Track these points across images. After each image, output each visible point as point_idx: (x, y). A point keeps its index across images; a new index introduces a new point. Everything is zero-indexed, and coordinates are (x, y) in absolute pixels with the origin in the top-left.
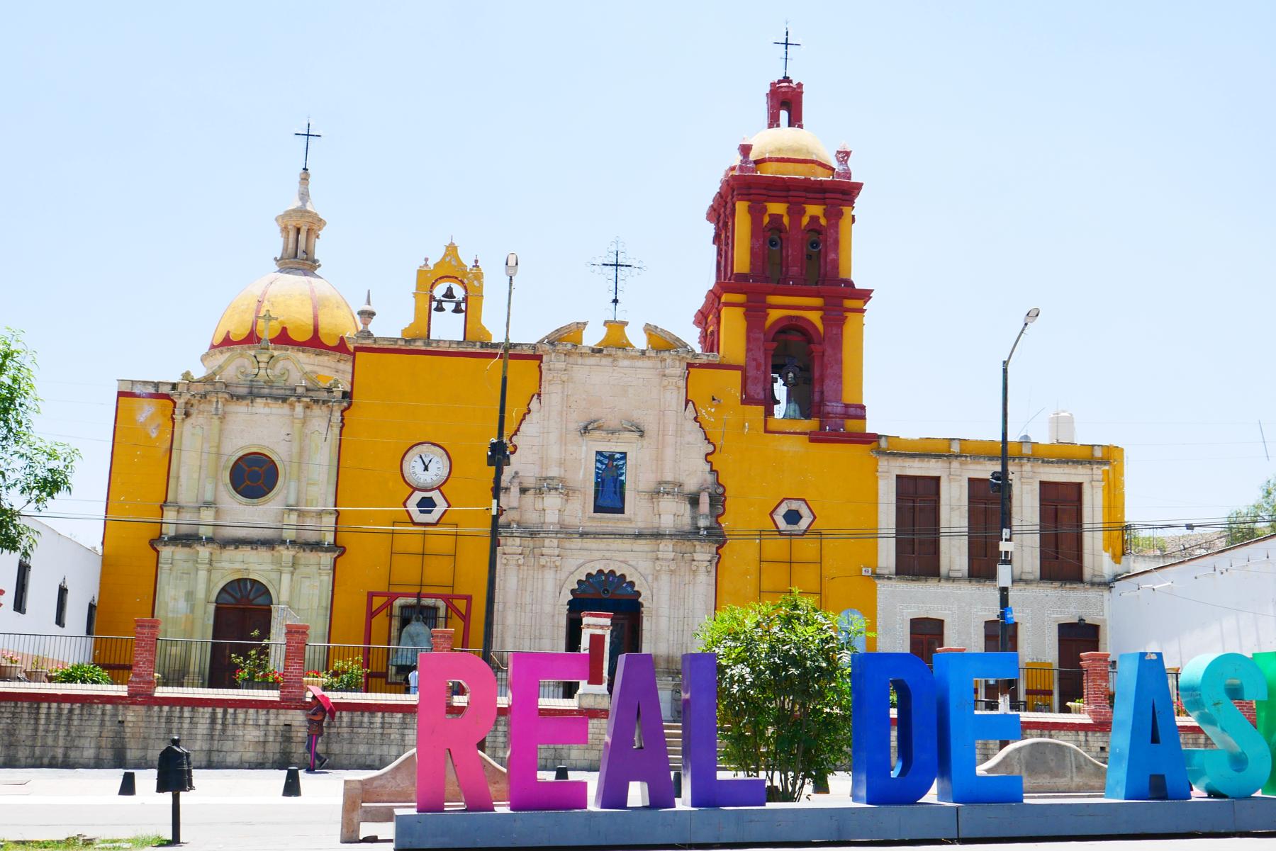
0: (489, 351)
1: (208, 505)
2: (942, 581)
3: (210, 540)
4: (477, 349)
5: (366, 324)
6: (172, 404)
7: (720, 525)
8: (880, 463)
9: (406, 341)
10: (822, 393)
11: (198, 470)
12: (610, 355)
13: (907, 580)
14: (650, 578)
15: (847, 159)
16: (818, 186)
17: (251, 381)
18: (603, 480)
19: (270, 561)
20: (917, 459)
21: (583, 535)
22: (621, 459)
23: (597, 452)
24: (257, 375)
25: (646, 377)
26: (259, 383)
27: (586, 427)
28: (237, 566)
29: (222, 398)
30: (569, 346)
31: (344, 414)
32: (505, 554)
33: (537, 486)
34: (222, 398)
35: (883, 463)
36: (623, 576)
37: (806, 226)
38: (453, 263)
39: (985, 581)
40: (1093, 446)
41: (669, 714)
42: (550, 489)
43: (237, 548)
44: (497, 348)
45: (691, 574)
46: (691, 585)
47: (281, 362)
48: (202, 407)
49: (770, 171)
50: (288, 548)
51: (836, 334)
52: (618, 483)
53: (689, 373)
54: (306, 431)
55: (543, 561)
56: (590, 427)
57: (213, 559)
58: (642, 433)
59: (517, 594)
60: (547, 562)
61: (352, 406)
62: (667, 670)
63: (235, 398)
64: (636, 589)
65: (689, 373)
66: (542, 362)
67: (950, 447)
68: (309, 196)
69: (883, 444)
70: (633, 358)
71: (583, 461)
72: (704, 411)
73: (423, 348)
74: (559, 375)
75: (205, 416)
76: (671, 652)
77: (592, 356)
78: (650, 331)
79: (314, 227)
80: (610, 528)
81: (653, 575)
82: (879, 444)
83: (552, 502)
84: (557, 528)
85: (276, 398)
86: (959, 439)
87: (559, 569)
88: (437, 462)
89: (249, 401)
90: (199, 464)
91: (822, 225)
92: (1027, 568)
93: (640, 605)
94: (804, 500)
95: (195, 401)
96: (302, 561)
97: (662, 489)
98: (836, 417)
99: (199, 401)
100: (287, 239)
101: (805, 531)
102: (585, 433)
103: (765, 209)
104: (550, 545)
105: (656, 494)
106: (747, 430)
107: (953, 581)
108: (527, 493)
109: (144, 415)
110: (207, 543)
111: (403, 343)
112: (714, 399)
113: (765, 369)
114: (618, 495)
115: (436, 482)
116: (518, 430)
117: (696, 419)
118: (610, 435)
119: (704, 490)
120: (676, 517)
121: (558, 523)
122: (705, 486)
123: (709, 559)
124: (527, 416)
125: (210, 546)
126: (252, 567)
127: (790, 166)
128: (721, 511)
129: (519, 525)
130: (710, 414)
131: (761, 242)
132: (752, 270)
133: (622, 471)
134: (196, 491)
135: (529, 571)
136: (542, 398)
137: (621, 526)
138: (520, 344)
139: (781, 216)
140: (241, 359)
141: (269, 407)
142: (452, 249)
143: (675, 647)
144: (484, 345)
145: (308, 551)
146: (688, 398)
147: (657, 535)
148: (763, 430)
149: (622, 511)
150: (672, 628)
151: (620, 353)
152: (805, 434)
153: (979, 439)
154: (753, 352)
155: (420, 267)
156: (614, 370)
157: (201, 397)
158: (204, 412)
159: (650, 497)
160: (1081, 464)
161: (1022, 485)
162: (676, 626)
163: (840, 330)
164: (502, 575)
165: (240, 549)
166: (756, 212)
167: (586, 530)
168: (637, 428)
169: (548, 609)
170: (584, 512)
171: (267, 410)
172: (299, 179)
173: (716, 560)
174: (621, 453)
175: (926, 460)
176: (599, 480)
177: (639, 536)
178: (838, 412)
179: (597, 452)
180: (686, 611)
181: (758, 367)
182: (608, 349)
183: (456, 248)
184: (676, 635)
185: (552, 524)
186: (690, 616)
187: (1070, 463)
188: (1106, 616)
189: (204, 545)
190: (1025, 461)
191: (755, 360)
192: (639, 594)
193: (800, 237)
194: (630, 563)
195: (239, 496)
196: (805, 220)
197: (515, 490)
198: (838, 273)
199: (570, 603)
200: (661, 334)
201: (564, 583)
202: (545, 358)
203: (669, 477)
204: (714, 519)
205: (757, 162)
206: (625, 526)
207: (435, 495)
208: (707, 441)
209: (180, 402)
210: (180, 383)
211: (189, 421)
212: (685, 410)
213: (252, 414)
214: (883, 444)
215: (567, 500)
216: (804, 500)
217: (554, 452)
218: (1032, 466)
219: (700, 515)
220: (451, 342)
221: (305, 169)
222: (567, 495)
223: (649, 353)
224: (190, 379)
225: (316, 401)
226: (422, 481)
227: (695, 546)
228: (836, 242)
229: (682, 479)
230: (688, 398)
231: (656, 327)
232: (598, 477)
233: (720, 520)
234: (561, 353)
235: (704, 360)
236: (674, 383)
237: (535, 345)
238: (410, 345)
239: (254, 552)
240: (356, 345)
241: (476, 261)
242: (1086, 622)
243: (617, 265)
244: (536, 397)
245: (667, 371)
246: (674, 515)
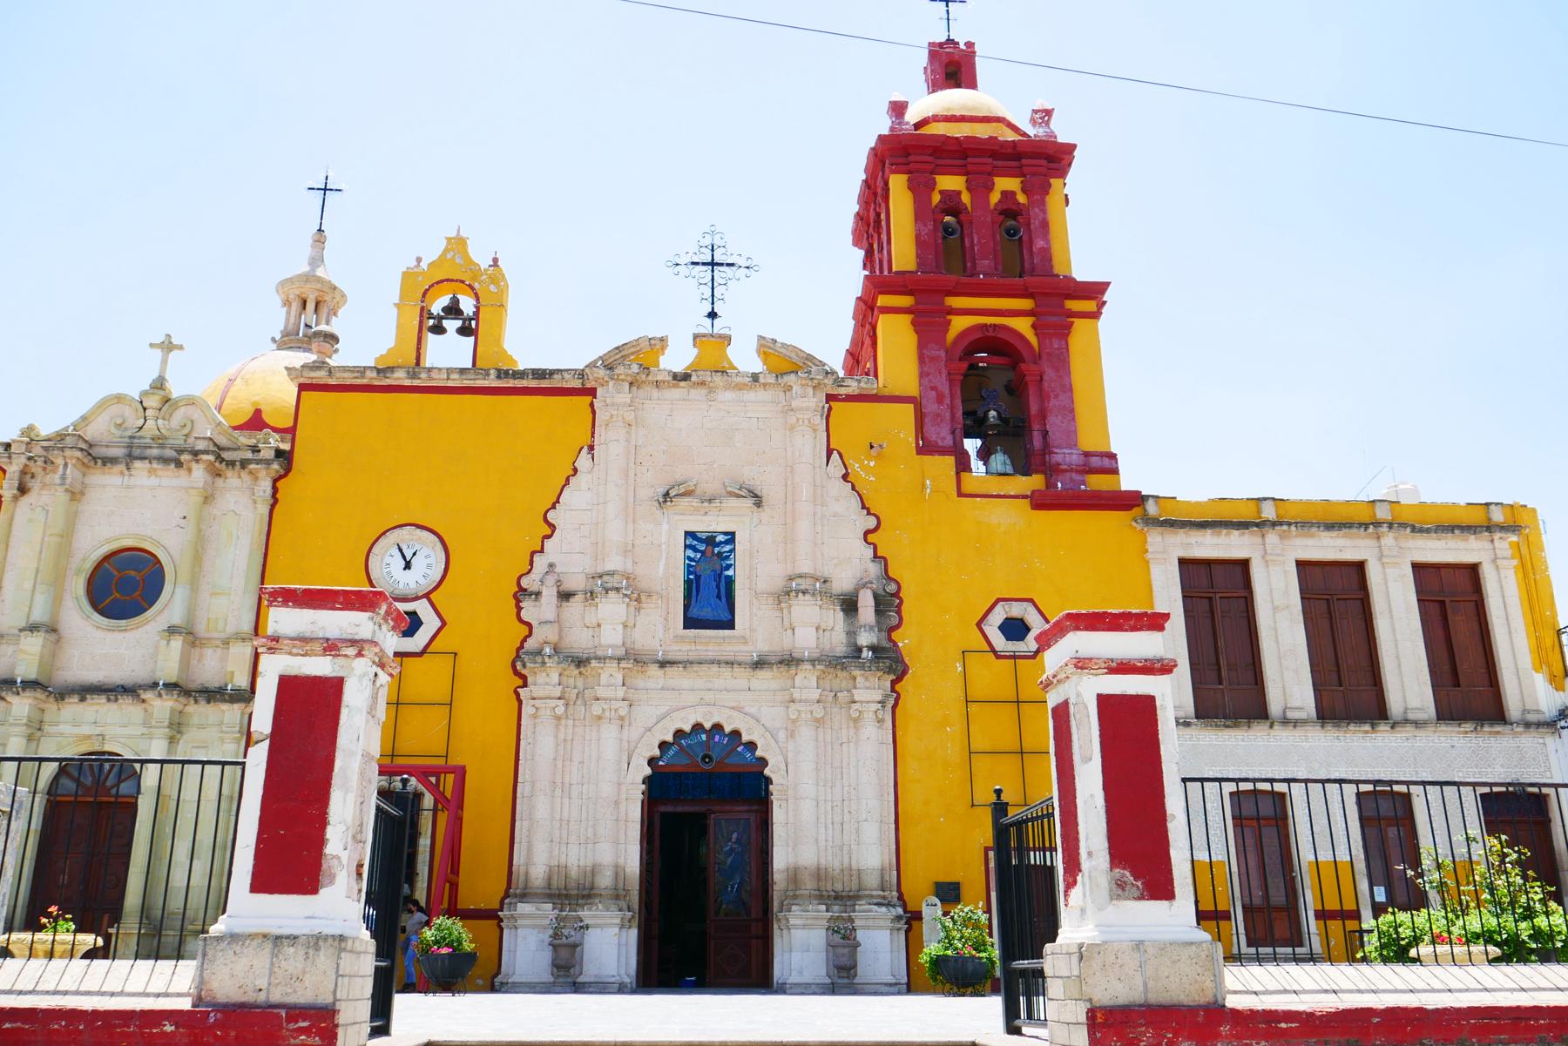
0: (511, 383)
1: (33, 628)
2: (1275, 727)
3: (31, 685)
4: (492, 382)
7: (895, 644)
8: (1149, 539)
9: (379, 371)
10: (1045, 434)
11: (33, 576)
12: (703, 383)
13: (1216, 726)
14: (782, 735)
16: (1009, 150)
17: (131, 437)
18: (698, 578)
19: (141, 722)
20: (1209, 531)
21: (663, 664)
22: (726, 542)
23: (687, 534)
24: (141, 428)
25: (763, 415)
27: (667, 494)
28: (86, 730)
29: (72, 458)
30: (635, 368)
31: (279, 484)
32: (534, 699)
33: (589, 588)
34: (72, 458)
36: (736, 734)
37: (996, 204)
38: (458, 261)
39: (1348, 724)
40: (1487, 504)
41: (824, 972)
42: (607, 590)
43: (83, 699)
44: (523, 378)
45: (851, 724)
46: (851, 744)
47: (183, 409)
48: (48, 479)
50: (160, 695)
51: (1057, 349)
52: (723, 580)
53: (830, 409)
54: (215, 511)
55: (596, 709)
56: (672, 493)
57: (45, 719)
58: (758, 500)
59: (555, 765)
60: (603, 709)
61: (290, 474)
62: (817, 893)
63: (99, 462)
64: (759, 753)
65: (830, 409)
67: (1259, 511)
68: (323, 261)
69: (1151, 508)
70: (740, 387)
71: (663, 546)
72: (857, 465)
73: (407, 382)
74: (621, 412)
76: (823, 862)
77: (675, 386)
78: (767, 348)
79: (326, 298)
80: (711, 654)
81: (786, 729)
82: (1145, 511)
83: (611, 610)
84: (621, 652)
85: (165, 460)
86: (1273, 499)
87: (627, 723)
88: (427, 557)
89: (122, 467)
90: (36, 566)
91: (1019, 203)
93: (768, 781)
94: (1031, 601)
95: (36, 468)
96: (195, 720)
97: (794, 585)
98: (1071, 470)
99: (44, 469)
102: (665, 501)
103: (935, 183)
104: (609, 677)
105: (786, 594)
106: (928, 491)
107: (1295, 727)
108: (571, 600)
110: (24, 690)
111: (374, 374)
112: (872, 447)
113: (951, 401)
114: (724, 599)
115: (424, 587)
116: (558, 501)
117: (845, 477)
118: (706, 504)
119: (864, 586)
120: (821, 631)
121: (623, 644)
122: (867, 580)
123: (880, 698)
125: (28, 693)
126: (110, 731)
128: (895, 621)
129: (556, 650)
130: (866, 469)
131: (931, 227)
132: (919, 265)
133: (728, 562)
134: (27, 609)
135: (577, 729)
136: (596, 452)
137: (728, 648)
139: (959, 193)
140: (120, 405)
141: (156, 476)
142: (457, 244)
143: (830, 852)
144: (502, 374)
145: (203, 703)
146: (832, 447)
147: (790, 661)
149: (730, 625)
150: (822, 820)
151: (718, 378)
152: (1024, 497)
153: (1304, 498)
154: (931, 377)
155: (408, 268)
156: (710, 406)
159: (776, 602)
160: (1475, 533)
161: (1384, 567)
162: (830, 816)
163: (1063, 343)
164: (529, 734)
165: (89, 701)
166: (920, 189)
167: (670, 657)
168: (749, 491)
169: (607, 790)
170: (666, 629)
171: (153, 481)
172: (311, 241)
173: (892, 701)
174: (726, 534)
175: (1225, 531)
176: (691, 577)
177: (759, 664)
178: (1073, 462)
179: (687, 534)
180: (846, 788)
181: (940, 400)
182: (699, 373)
184: (830, 831)
185: (613, 647)
186: (853, 797)
187: (1456, 531)
189: (18, 694)
190: (1384, 529)
191: (933, 388)
192: (763, 762)
193: (989, 220)
194: (747, 709)
195: (97, 616)
196: (995, 198)
197: (549, 594)
198: (1052, 267)
199: (648, 781)
200: (783, 351)
201: (636, 747)
203: (805, 568)
204: (884, 634)
205: (918, 126)
206: (736, 648)
207: (422, 608)
208: (865, 512)
210: (14, 441)
211: (25, 500)
212: (827, 465)
213: (128, 487)
214: (1151, 508)
215: (638, 610)
216: (1031, 601)
217: (615, 532)
218: (1396, 538)
219: (860, 628)
220: (449, 371)
221: (320, 230)
222: (638, 600)
223: (765, 378)
224: (33, 436)
225: (231, 464)
226: (401, 586)
227: (854, 678)
228: (1045, 225)
229: (826, 571)
230: (832, 447)
231: (775, 341)
232: (689, 573)
233: (894, 635)
234: (623, 380)
235: (853, 387)
236: (806, 422)
237: (583, 370)
238: (388, 378)
239: (113, 706)
240: (302, 380)
241: (495, 260)
243: (713, 264)
244: (585, 449)
245: (794, 404)
246: (817, 629)
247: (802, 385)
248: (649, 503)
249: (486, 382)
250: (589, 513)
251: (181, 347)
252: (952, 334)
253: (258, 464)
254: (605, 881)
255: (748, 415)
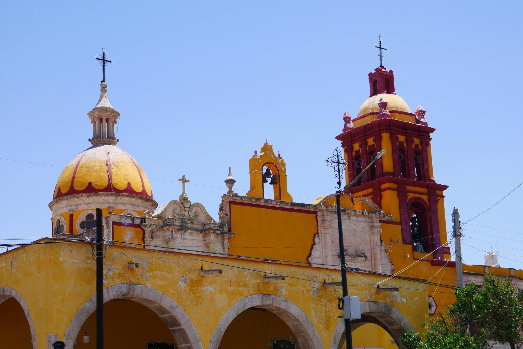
5: (230, 188)
6: (142, 232)
12: (348, 214)
15: (424, 115)
17: (182, 219)
26: (185, 220)
49: (397, 118)
66: (317, 216)
67: (485, 270)
73: (263, 204)
74: (330, 224)
75: (160, 239)
89: (183, 231)
91: (420, 150)
100: (94, 126)
109: (128, 237)
124: (314, 246)
127: (404, 116)
130: (390, 248)
138: (309, 205)
139: (403, 143)
141: (192, 235)
144: (293, 204)
148: (412, 259)
151: (353, 213)
152: (429, 261)
156: (350, 222)
157: (160, 228)
158: (160, 237)
166: (393, 139)
171: (191, 237)
183: (271, 147)
191: (405, 220)
202: (319, 214)
209: (147, 230)
213: (184, 239)
234: (329, 211)
236: (378, 231)
237: (316, 205)
238: (258, 202)
240: (231, 200)
247: (376, 218)
248: (336, 256)
249: (287, 206)
250: (320, 259)
251: (188, 181)
252: (408, 200)
253: (227, 234)
255: (360, 226)
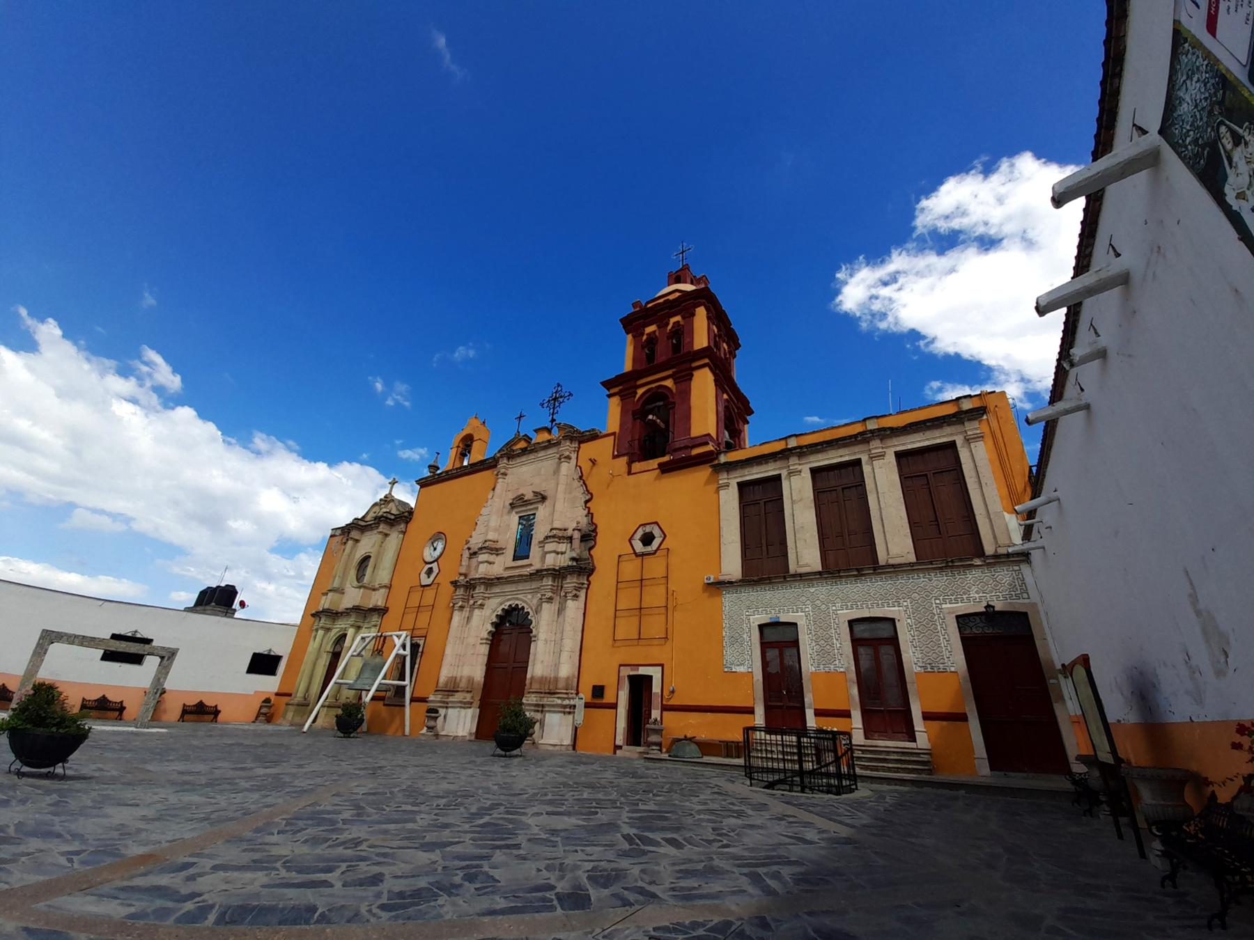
35: (723, 478)
92: (894, 550)
101: (656, 551)
188: (1035, 597)
216: (656, 523)
242: (996, 609)
254: (463, 684)
